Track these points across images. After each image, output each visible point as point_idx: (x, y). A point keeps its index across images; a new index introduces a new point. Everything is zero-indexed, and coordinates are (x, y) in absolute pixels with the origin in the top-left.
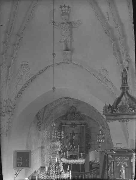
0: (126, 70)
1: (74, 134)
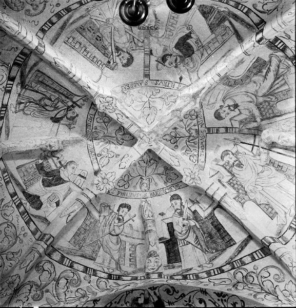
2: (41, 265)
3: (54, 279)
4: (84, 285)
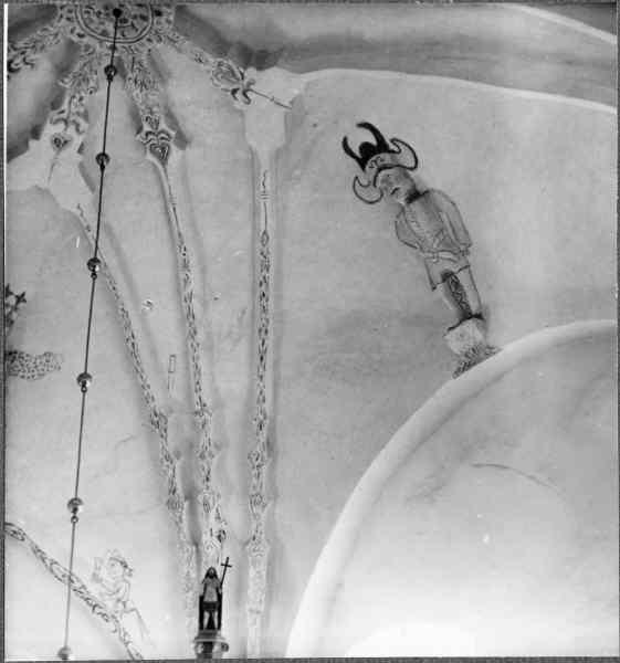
0: (219, 575)
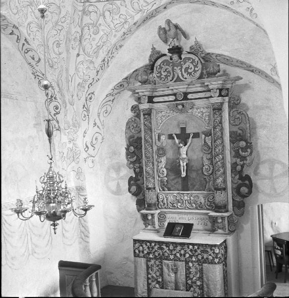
1: (184, 137)
2: (87, 9)
3: (100, 15)
4: (123, 10)
